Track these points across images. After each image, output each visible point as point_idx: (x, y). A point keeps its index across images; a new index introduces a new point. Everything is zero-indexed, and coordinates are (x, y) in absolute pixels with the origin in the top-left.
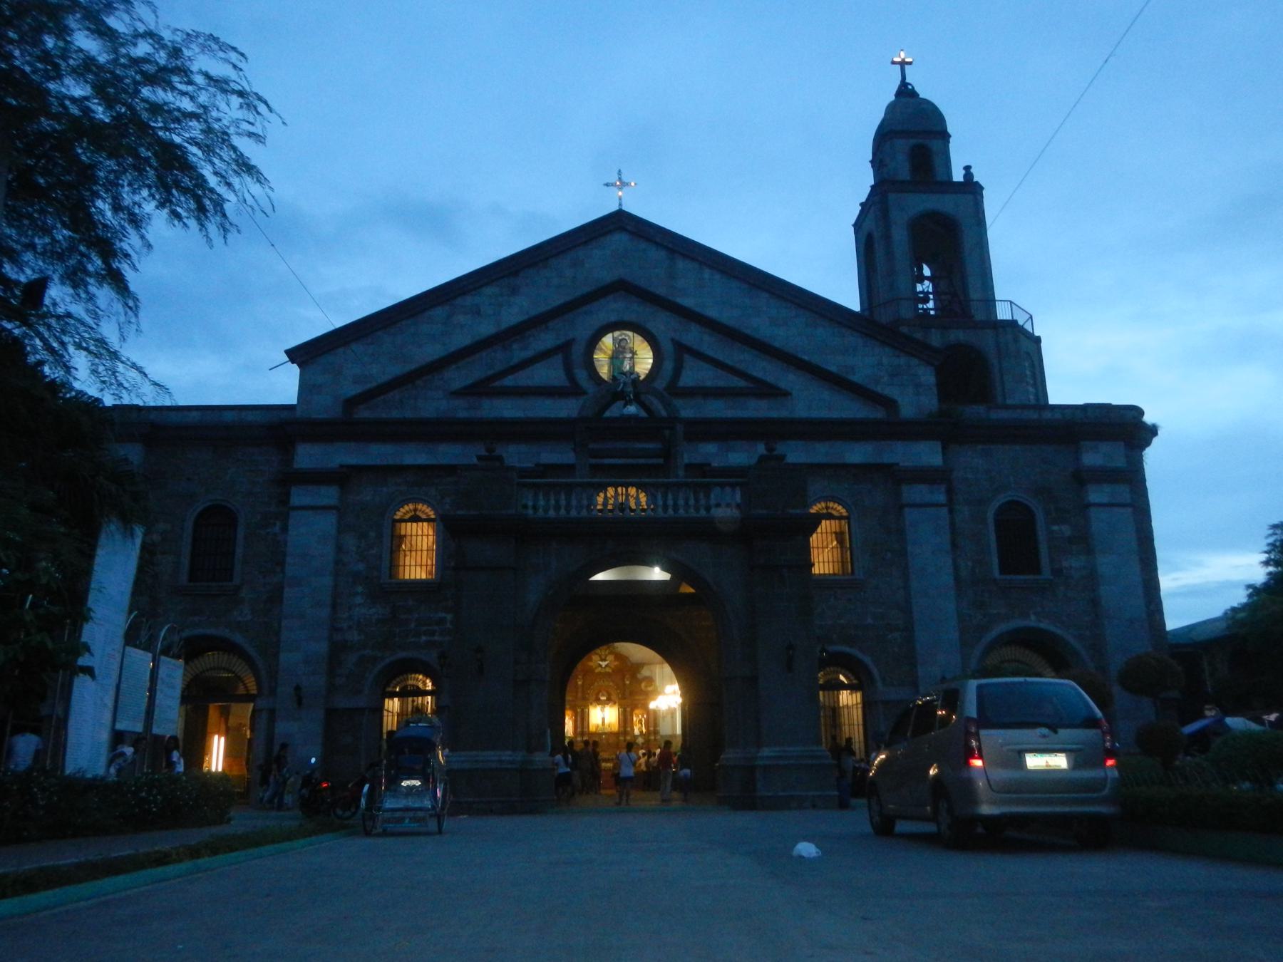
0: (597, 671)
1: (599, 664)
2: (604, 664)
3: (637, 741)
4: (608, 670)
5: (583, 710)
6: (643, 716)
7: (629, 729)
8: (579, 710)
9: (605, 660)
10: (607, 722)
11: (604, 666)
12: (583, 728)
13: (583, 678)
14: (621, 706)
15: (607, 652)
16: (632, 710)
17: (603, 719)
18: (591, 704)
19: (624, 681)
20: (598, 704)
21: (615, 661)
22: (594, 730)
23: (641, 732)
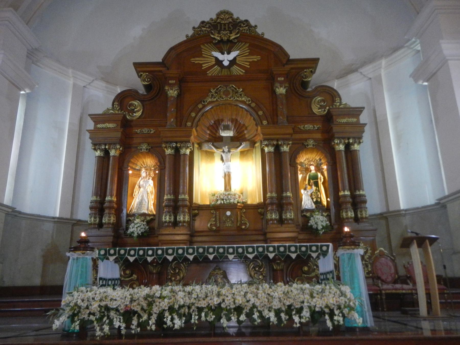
0: (209, 73)
1: (216, 59)
2: (226, 59)
3: (312, 222)
4: (236, 70)
5: (177, 150)
6: (319, 168)
7: (289, 194)
8: (169, 151)
9: (229, 53)
10: (236, 187)
11: (226, 63)
12: (176, 192)
13: (180, 88)
14: (268, 139)
15: (233, 37)
16: (294, 155)
17: (227, 177)
18: (200, 146)
19: (274, 92)
20: (217, 148)
21: (251, 54)
22: (208, 203)
23: (318, 203)
